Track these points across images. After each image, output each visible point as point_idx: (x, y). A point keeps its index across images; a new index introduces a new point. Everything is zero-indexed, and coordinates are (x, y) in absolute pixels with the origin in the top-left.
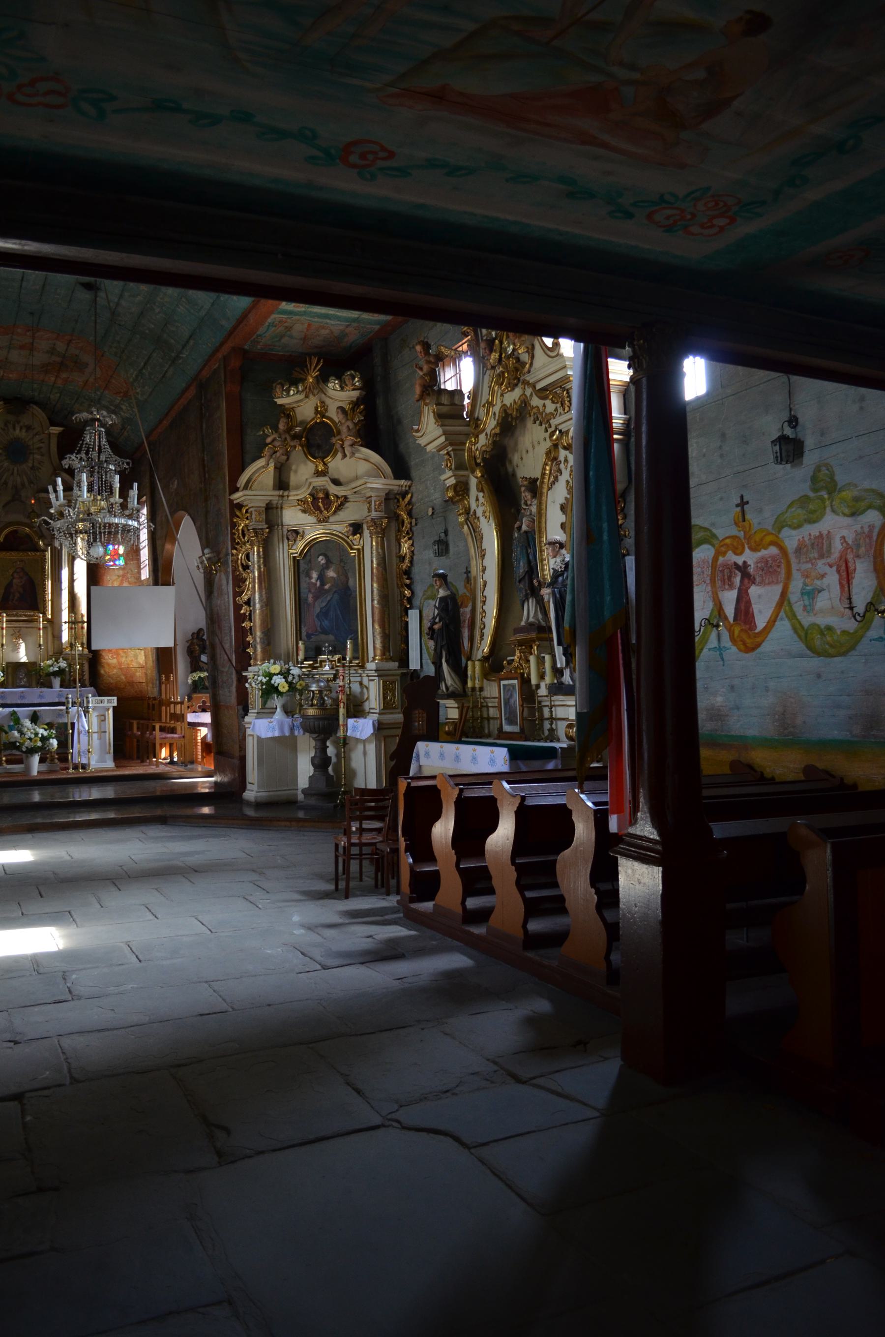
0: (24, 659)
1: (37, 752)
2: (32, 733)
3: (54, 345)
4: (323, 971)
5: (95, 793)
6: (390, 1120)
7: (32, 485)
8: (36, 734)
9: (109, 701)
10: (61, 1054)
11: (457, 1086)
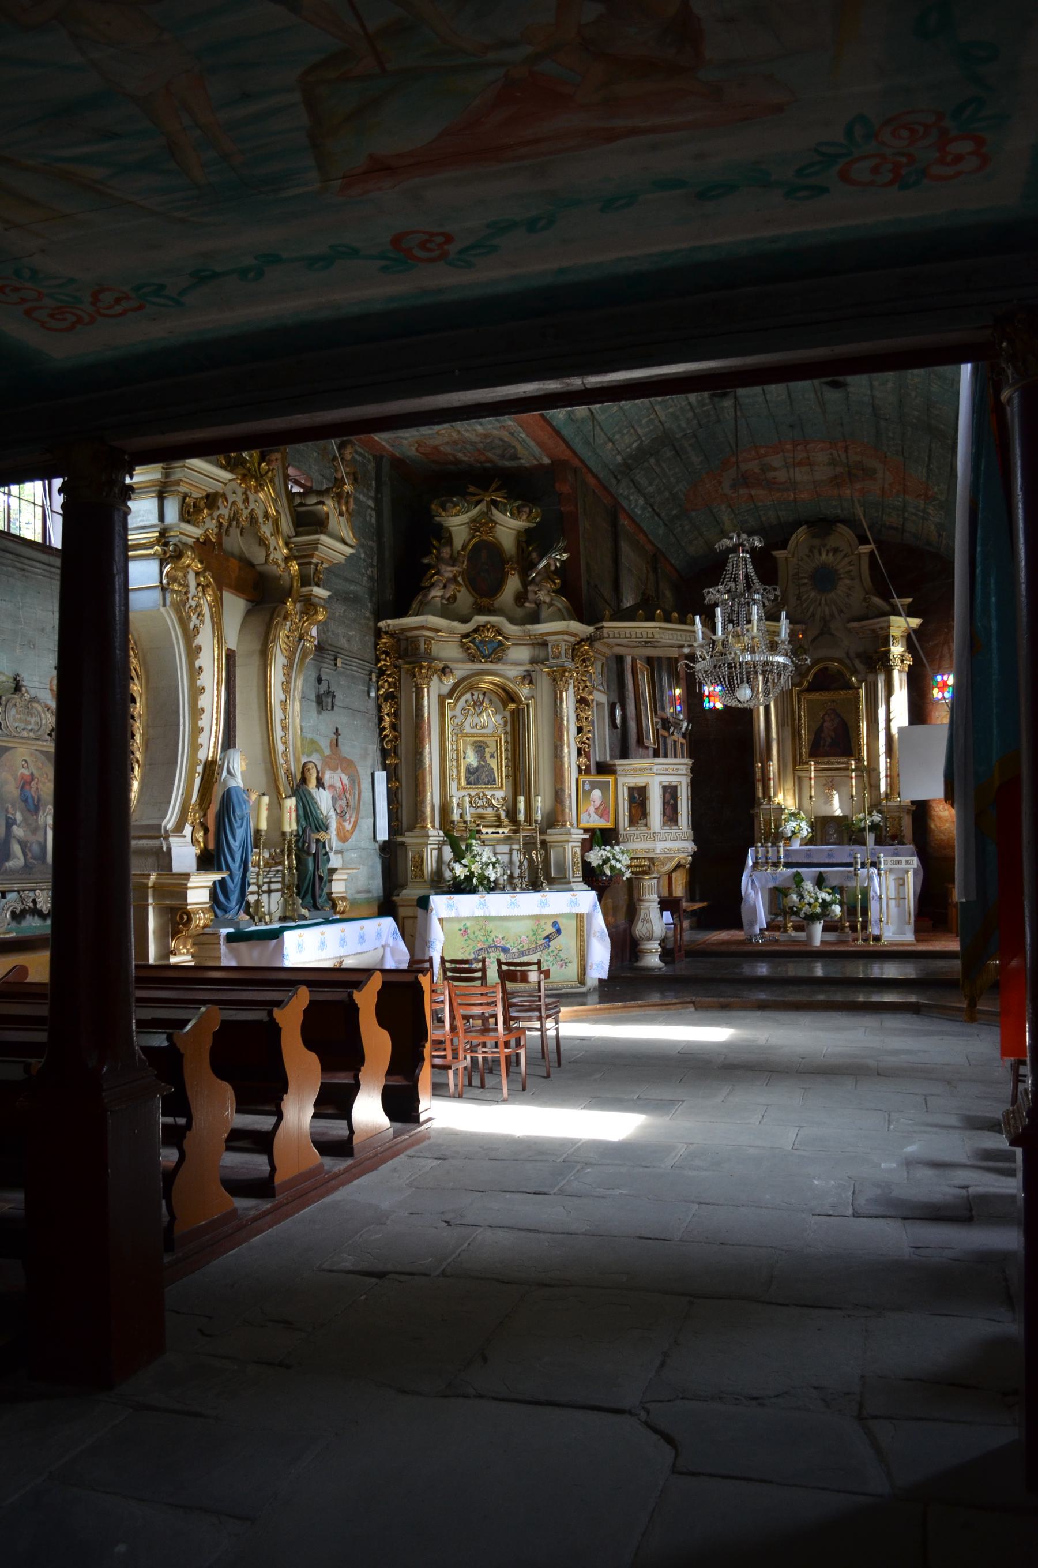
0: (838, 813)
1: (819, 919)
2: (812, 897)
3: (832, 454)
4: (853, 1219)
5: (891, 971)
6: (643, 1408)
7: (842, 615)
8: (817, 899)
9: (907, 862)
10: (466, 1245)
11: (777, 1396)
